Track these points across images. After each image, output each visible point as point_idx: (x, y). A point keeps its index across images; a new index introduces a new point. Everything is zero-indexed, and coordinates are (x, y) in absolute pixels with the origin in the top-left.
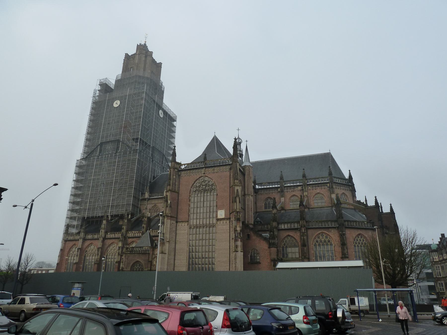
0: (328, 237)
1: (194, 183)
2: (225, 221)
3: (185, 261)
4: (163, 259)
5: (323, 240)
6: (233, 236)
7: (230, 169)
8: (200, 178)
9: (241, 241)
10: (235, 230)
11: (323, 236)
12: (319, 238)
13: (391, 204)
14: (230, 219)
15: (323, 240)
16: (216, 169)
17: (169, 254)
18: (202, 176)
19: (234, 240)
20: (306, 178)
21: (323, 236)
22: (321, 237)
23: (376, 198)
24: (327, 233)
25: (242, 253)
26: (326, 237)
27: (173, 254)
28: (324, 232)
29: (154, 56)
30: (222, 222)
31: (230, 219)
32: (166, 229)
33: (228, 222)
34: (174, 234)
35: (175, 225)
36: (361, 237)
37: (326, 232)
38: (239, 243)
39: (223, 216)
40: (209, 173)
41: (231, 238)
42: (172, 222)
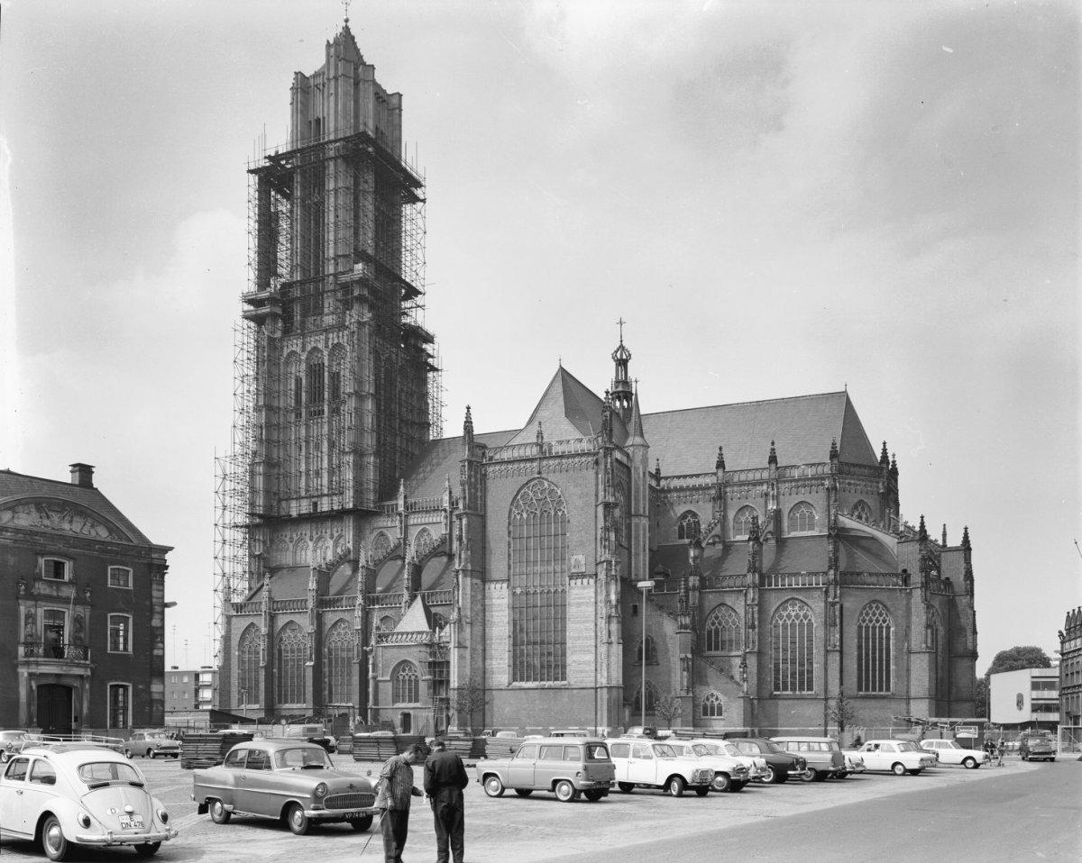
1: (517, 495)
3: (507, 661)
4: (461, 657)
5: (793, 614)
6: (603, 611)
9: (618, 622)
12: (785, 609)
13: (966, 529)
14: (596, 575)
15: (793, 614)
17: (473, 650)
18: (534, 479)
20: (777, 464)
25: (621, 646)
26: (801, 608)
27: (480, 647)
28: (797, 597)
29: (379, 77)
31: (596, 577)
32: (463, 597)
33: (592, 581)
34: (479, 607)
35: (481, 587)
37: (801, 598)
38: (614, 627)
41: (599, 616)
42: (475, 581)
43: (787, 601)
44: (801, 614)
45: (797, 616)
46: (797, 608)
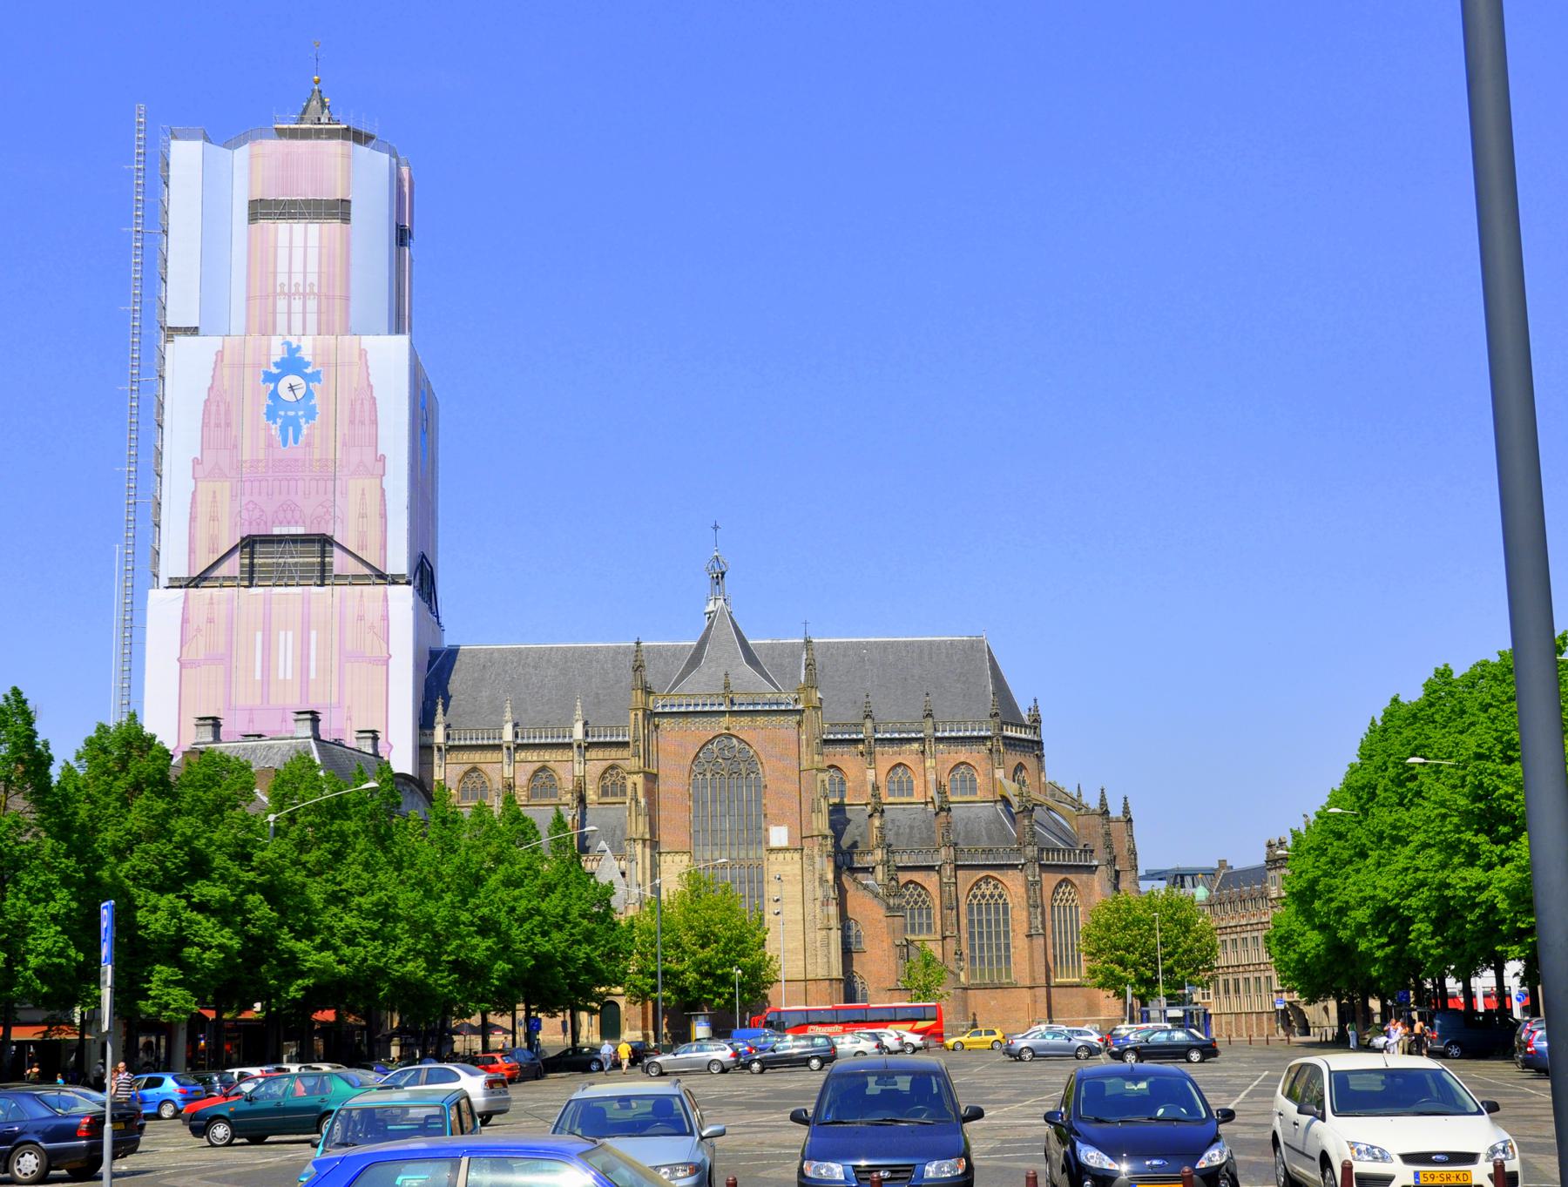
0: (1000, 886)
2: (788, 855)
7: (799, 724)
8: (714, 738)
10: (822, 881)
11: (987, 883)
13: (1125, 798)
14: (802, 849)
15: (988, 893)
16: (761, 720)
19: (818, 903)
21: (987, 883)
22: (984, 886)
23: (1103, 792)
24: (999, 877)
26: (996, 887)
30: (781, 856)
36: (1066, 886)
39: (785, 843)
40: (742, 728)
43: (980, 880)
44: (996, 893)
45: (992, 896)
46: (991, 886)
